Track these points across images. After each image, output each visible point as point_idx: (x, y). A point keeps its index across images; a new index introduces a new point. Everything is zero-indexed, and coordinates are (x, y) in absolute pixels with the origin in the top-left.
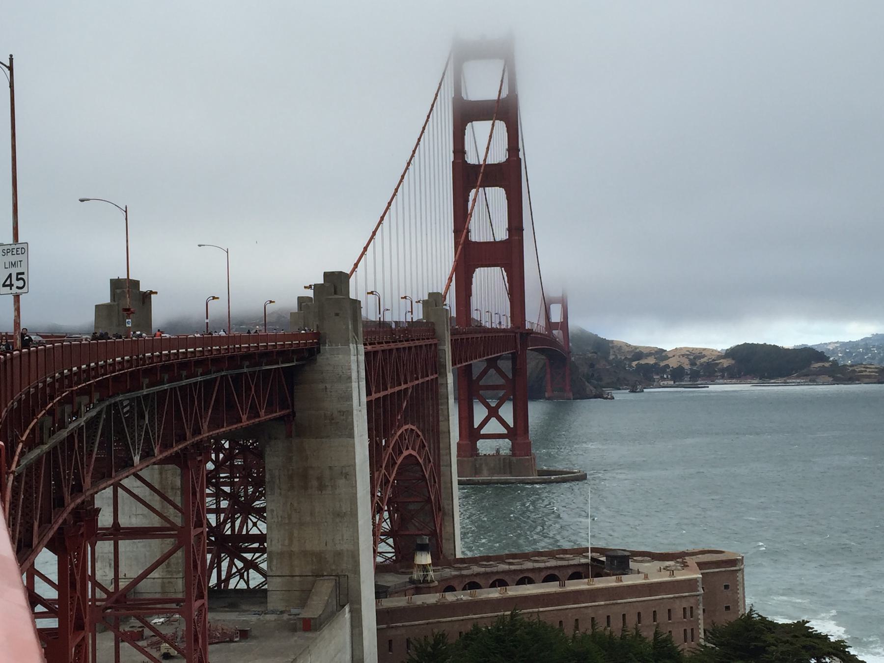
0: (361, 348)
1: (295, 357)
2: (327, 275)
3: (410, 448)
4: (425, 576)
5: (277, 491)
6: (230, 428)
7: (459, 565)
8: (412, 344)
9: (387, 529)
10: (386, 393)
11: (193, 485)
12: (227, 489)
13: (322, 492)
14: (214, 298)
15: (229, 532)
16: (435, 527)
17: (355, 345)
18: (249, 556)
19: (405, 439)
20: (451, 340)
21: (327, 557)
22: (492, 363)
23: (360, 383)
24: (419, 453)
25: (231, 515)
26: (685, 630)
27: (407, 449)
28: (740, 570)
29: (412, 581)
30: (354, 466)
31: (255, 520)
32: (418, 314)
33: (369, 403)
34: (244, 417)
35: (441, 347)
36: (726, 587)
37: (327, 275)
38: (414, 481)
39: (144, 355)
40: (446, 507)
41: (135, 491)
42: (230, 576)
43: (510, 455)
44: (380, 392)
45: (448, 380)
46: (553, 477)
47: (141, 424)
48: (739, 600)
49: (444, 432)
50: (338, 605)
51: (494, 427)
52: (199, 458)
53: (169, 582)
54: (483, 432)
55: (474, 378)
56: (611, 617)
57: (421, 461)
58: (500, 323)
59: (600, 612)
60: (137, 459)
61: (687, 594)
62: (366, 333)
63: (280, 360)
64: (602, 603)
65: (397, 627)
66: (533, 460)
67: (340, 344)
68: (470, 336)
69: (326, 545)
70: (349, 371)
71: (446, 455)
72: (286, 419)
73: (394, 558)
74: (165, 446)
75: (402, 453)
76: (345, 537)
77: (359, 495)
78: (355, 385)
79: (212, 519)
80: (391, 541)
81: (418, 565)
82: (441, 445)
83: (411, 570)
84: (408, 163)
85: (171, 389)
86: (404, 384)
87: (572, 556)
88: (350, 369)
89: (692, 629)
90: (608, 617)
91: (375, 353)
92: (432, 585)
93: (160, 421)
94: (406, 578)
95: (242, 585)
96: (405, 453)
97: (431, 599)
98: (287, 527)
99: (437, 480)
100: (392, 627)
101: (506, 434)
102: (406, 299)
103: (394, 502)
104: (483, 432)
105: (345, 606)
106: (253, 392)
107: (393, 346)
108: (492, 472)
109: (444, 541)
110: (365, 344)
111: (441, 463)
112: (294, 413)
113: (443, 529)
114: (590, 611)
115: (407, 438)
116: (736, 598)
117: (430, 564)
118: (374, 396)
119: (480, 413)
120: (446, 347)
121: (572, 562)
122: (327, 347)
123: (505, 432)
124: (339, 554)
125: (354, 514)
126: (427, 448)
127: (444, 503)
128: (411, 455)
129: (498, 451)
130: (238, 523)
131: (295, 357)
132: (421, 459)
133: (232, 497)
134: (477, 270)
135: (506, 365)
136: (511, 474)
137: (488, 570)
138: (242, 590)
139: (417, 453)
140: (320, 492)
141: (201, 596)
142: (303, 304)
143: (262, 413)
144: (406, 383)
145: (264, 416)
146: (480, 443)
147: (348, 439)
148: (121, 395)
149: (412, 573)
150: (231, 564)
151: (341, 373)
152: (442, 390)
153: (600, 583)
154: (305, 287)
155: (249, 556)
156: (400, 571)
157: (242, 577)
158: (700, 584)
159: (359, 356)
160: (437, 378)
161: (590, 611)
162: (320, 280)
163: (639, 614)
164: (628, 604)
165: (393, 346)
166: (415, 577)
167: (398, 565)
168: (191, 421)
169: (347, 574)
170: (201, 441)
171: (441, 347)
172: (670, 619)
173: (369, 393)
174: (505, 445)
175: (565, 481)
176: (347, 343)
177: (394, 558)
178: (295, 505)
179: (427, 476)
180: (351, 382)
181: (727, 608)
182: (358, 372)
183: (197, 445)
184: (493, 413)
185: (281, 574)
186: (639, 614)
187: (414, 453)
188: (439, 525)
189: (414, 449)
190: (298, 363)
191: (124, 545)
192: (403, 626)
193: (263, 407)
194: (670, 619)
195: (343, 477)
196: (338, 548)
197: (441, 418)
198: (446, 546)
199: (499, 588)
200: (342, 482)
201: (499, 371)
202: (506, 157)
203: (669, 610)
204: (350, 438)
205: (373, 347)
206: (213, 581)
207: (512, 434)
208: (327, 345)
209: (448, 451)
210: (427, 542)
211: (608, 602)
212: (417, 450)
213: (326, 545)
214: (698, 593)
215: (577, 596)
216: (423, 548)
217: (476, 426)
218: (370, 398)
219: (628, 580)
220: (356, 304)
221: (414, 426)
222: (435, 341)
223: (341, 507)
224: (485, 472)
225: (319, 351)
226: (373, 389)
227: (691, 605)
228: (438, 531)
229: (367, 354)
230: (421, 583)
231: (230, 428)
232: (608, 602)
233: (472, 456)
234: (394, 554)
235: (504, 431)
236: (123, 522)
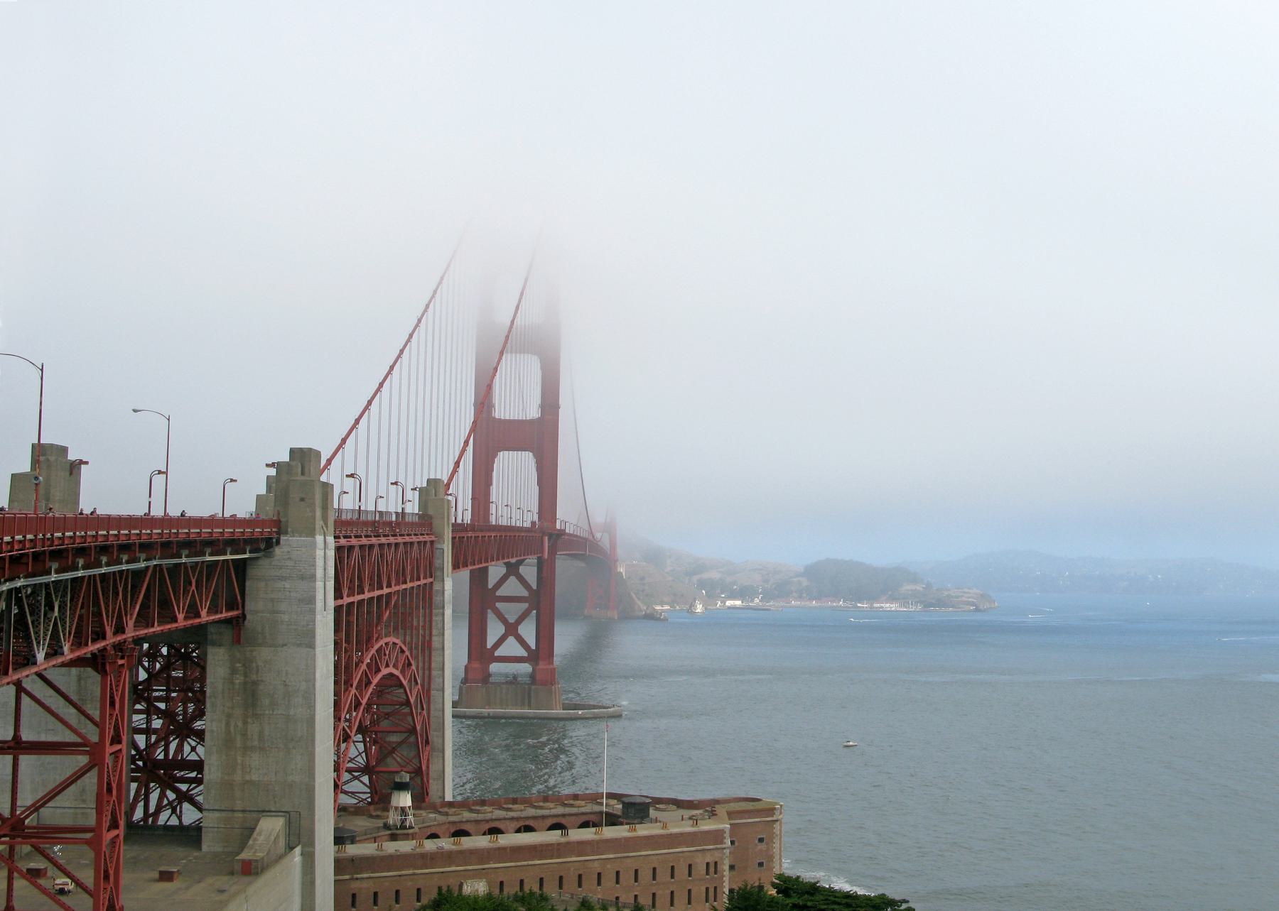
0: (331, 539)
1: (248, 549)
2: (293, 452)
3: (391, 666)
4: (403, 821)
6: (162, 628)
7: (446, 809)
8: (400, 540)
10: (361, 597)
11: (112, 693)
12: (162, 706)
13: (273, 711)
15: (161, 757)
16: (421, 763)
18: (184, 787)
19: (385, 655)
20: (453, 538)
21: (276, 789)
22: (513, 570)
23: (327, 583)
24: (403, 672)
25: (164, 737)
26: (707, 889)
27: (387, 666)
28: (777, 821)
29: (386, 827)
31: (194, 744)
32: (413, 508)
33: (338, 610)
34: (181, 616)
35: (438, 546)
36: (761, 840)
37: (293, 452)
38: (397, 707)
39: (52, 535)
40: (435, 739)
41: (47, 702)
42: (159, 808)
44: (354, 596)
45: (446, 586)
47: (49, 616)
48: (774, 855)
49: (437, 649)
50: (287, 848)
51: (511, 648)
52: (120, 662)
53: (83, 813)
54: (497, 653)
56: (621, 873)
57: (405, 682)
59: (609, 866)
60: (40, 656)
61: (711, 847)
62: (339, 523)
63: (229, 550)
64: (611, 856)
65: (362, 878)
68: (480, 534)
70: (313, 568)
71: (439, 678)
72: (234, 622)
73: (369, 800)
74: (79, 642)
77: (318, 717)
78: (319, 584)
79: (141, 740)
80: (366, 779)
81: (396, 808)
82: (433, 665)
83: (386, 814)
85: (90, 576)
86: (387, 587)
87: (584, 802)
88: (314, 565)
89: (715, 888)
90: (618, 873)
91: (351, 548)
92: (411, 831)
93: (72, 615)
94: (380, 823)
95: (174, 821)
96: (385, 671)
97: (405, 847)
99: (425, 707)
100: (357, 879)
102: (397, 485)
103: (371, 732)
104: (497, 653)
105: (294, 848)
106: (194, 587)
107: (374, 541)
109: (431, 781)
110: (335, 537)
111: (432, 686)
113: (430, 766)
114: (596, 864)
115: (387, 652)
116: (771, 853)
117: (409, 807)
118: (347, 600)
119: (494, 631)
121: (583, 810)
123: (524, 654)
126: (414, 667)
127: (433, 736)
128: (391, 675)
130: (173, 746)
131: (248, 549)
132: (405, 679)
133: (168, 715)
135: (529, 571)
137: (480, 817)
138: (173, 827)
139: (401, 672)
140: (271, 712)
141: (115, 825)
143: (204, 613)
144: (389, 586)
145: (205, 617)
146: (494, 667)
147: (308, 649)
148: (22, 580)
149: (388, 817)
150: (162, 795)
152: (438, 598)
153: (609, 832)
154: (267, 465)
155: (184, 787)
156: (374, 814)
157: (174, 811)
158: (727, 835)
160: (432, 582)
161: (596, 864)
162: (286, 458)
163: (654, 869)
164: (641, 858)
165: (374, 541)
166: (391, 821)
167: (372, 808)
168: (113, 617)
170: (125, 642)
171: (438, 546)
172: (690, 875)
173: (338, 594)
175: (595, 718)
176: (312, 533)
177: (369, 800)
179: (412, 701)
180: (315, 581)
181: (761, 864)
182: (325, 569)
183: (119, 647)
184: (511, 629)
185: (219, 808)
186: (654, 869)
187: (397, 672)
188: (425, 762)
189: (395, 666)
191: (26, 760)
192: (370, 878)
193: (205, 605)
194: (690, 875)
196: (290, 778)
197: (435, 632)
198: (433, 787)
199: (489, 836)
203: (690, 866)
205: (348, 541)
206: (139, 814)
209: (440, 672)
210: (408, 780)
211: (619, 855)
212: (400, 667)
214: (724, 846)
215: (581, 847)
216: (401, 787)
217: (489, 646)
218: (340, 602)
219: (643, 830)
220: (327, 487)
221: (398, 638)
222: (433, 538)
225: (278, 543)
226: (345, 592)
227: (716, 860)
228: (424, 768)
229: (339, 549)
230: (397, 829)
231: (162, 628)
232: (619, 855)
234: (369, 795)
235: (524, 654)
236: (26, 736)
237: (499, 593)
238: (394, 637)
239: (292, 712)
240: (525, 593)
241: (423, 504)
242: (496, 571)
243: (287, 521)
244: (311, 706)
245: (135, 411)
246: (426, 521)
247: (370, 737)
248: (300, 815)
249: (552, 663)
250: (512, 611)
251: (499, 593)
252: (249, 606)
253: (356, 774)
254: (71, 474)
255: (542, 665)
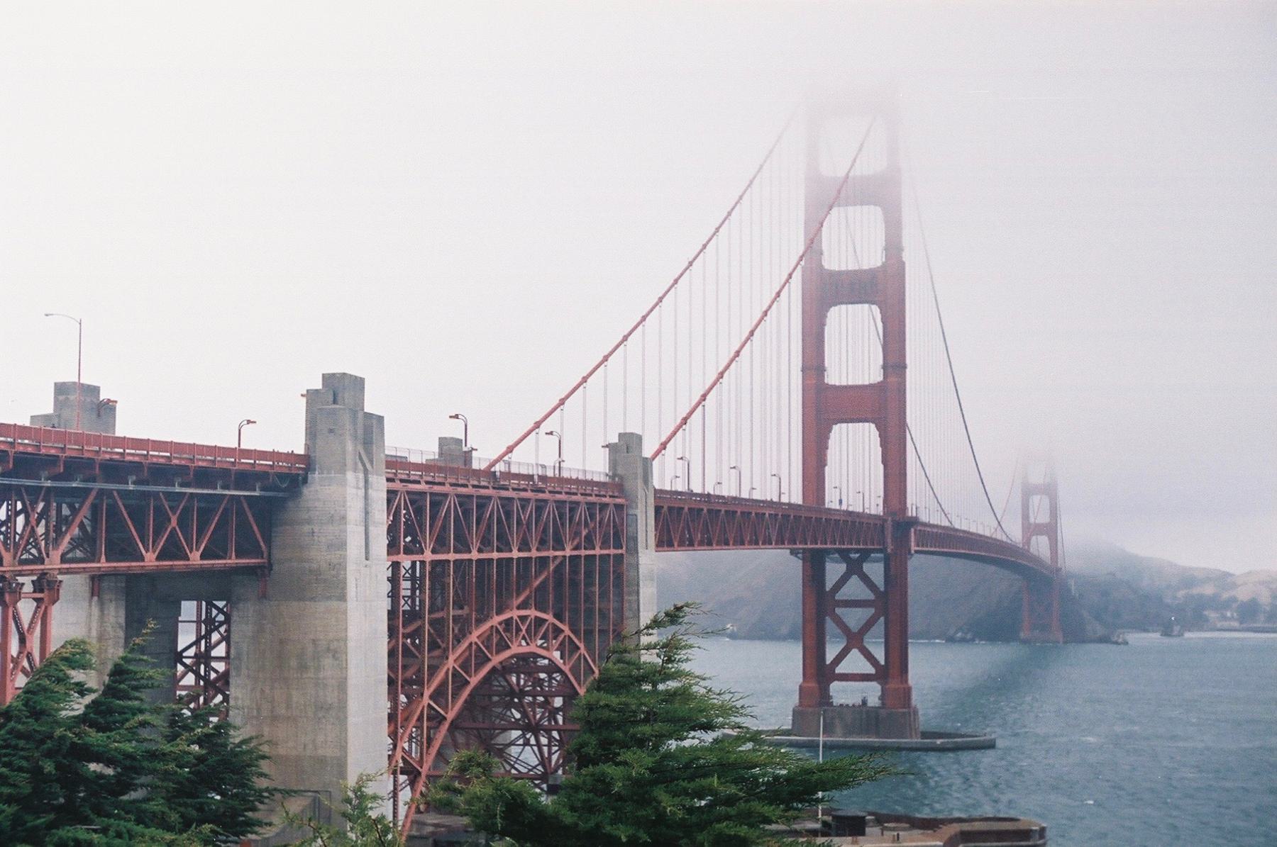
1: (258, 485)
5: (244, 671)
9: (540, 771)
14: (249, 422)
17: (361, 476)
22: (855, 568)
30: (345, 640)
35: (631, 512)
43: (879, 707)
44: (449, 553)
46: (939, 742)
51: (855, 663)
54: (839, 670)
55: (829, 585)
58: (841, 502)
63: (219, 483)
66: (912, 714)
67: (333, 472)
69: (305, 748)
72: (259, 571)
75: (509, 647)
76: (329, 739)
84: (689, 263)
98: (254, 722)
101: (872, 674)
104: (839, 670)
108: (849, 731)
110: (388, 480)
112: (270, 565)
115: (524, 628)
120: (639, 511)
122: (316, 475)
123: (872, 671)
124: (322, 761)
125: (342, 706)
129: (864, 702)
134: (836, 428)
135: (875, 570)
136: (878, 735)
142: (445, 447)
145: (195, 558)
146: (835, 687)
147: (339, 602)
151: (332, 512)
159: (370, 491)
169: (329, 790)
171: (631, 512)
174: (872, 693)
175: (957, 748)
176: (342, 469)
178: (267, 691)
182: (367, 513)
184: (855, 640)
190: (263, 493)
195: (330, 655)
196: (320, 752)
197: (627, 614)
200: (327, 661)
201: (866, 579)
202: (881, 260)
204: (340, 600)
207: (881, 674)
208: (317, 473)
213: (305, 748)
217: (828, 662)
221: (548, 614)
222: (619, 501)
223: (326, 696)
224: (839, 730)
225: (305, 481)
233: (820, 704)
235: (872, 671)
237: (839, 596)
238: (537, 608)
239: (321, 676)
240: (871, 596)
241: (613, 464)
242: (834, 570)
243: (315, 456)
244: (343, 668)
245: (47, 315)
246: (616, 485)
247: (550, 738)
248: (330, 795)
249: (906, 681)
250: (854, 618)
251: (838, 597)
252: (277, 554)
253: (537, 782)
254: (99, 415)
255: (893, 684)
